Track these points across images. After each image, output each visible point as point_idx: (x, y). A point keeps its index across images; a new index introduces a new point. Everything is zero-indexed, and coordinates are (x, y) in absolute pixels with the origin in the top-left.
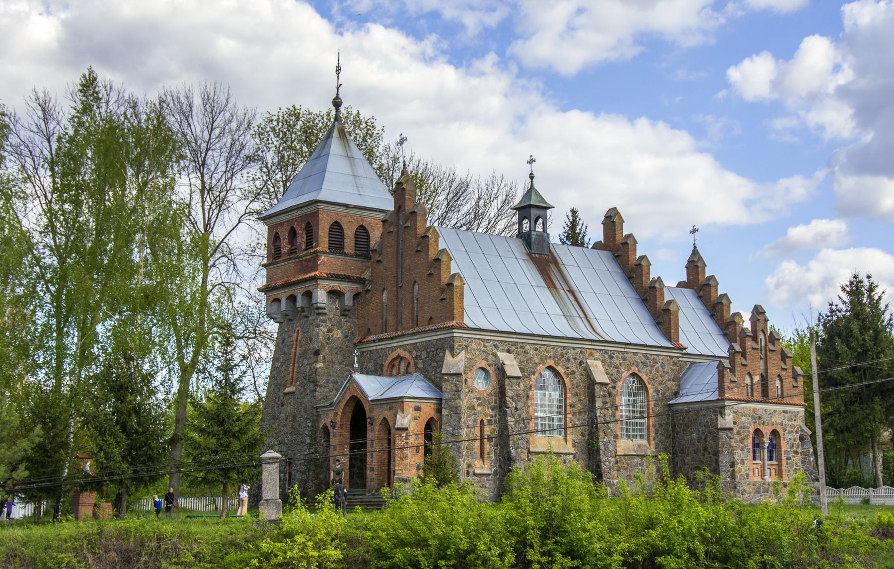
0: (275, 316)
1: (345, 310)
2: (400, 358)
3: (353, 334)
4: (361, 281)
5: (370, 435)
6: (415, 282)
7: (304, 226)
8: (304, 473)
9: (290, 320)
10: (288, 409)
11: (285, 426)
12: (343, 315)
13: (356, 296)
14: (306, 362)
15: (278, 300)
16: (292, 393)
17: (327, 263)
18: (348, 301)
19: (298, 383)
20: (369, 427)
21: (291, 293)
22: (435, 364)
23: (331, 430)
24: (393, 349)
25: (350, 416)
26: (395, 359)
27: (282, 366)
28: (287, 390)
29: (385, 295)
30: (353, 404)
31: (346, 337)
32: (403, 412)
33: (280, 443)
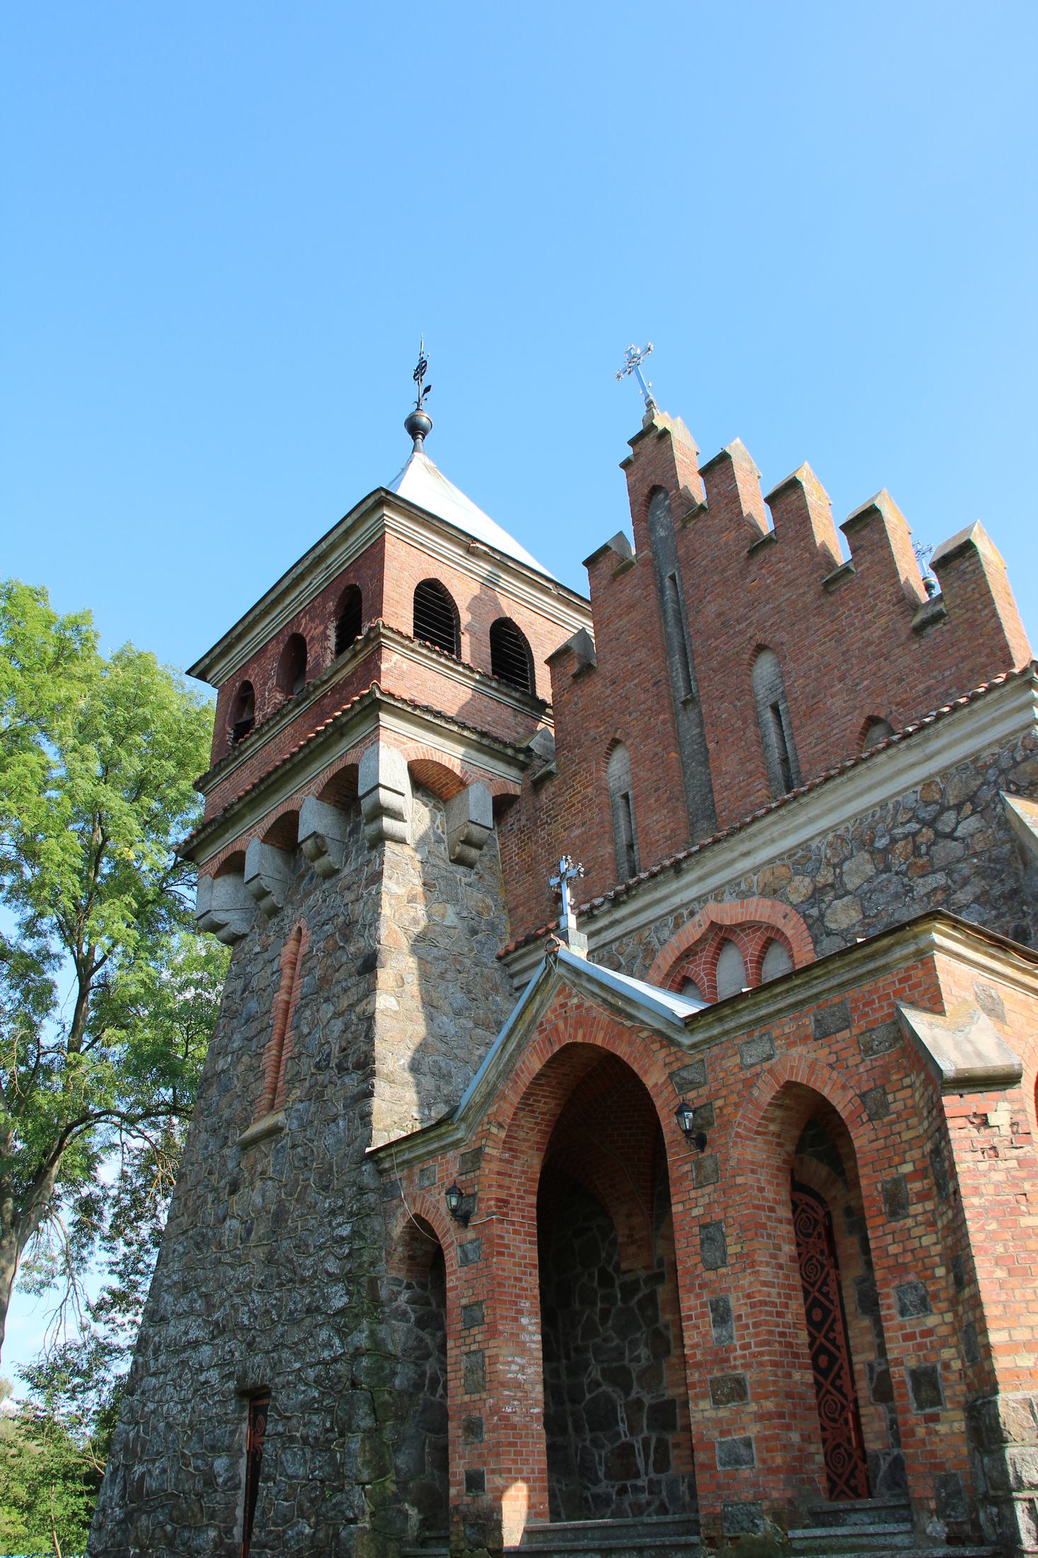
0: (219, 917)
1: (468, 842)
2: (722, 936)
3: (493, 926)
4: (519, 757)
5: (690, 1205)
6: (761, 648)
7: (331, 605)
8: (320, 1445)
9: (274, 911)
10: (255, 1196)
11: (239, 1262)
12: (459, 861)
13: (502, 805)
14: (327, 1010)
15: (234, 864)
16: (274, 1131)
17: (405, 671)
18: (478, 805)
19: (297, 1093)
20: (679, 1160)
21: (281, 811)
22: (940, 879)
23: (452, 1238)
24: (678, 918)
25: (533, 1162)
26: (688, 954)
27: (234, 1064)
28: (255, 1129)
29: (618, 768)
30: (547, 1105)
31: (474, 932)
32: (934, 1004)
33: (219, 1330)
